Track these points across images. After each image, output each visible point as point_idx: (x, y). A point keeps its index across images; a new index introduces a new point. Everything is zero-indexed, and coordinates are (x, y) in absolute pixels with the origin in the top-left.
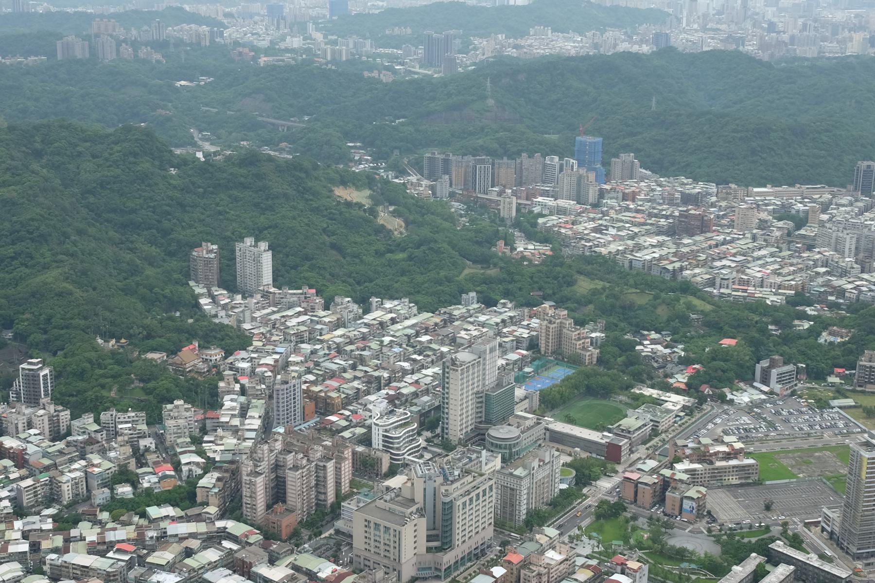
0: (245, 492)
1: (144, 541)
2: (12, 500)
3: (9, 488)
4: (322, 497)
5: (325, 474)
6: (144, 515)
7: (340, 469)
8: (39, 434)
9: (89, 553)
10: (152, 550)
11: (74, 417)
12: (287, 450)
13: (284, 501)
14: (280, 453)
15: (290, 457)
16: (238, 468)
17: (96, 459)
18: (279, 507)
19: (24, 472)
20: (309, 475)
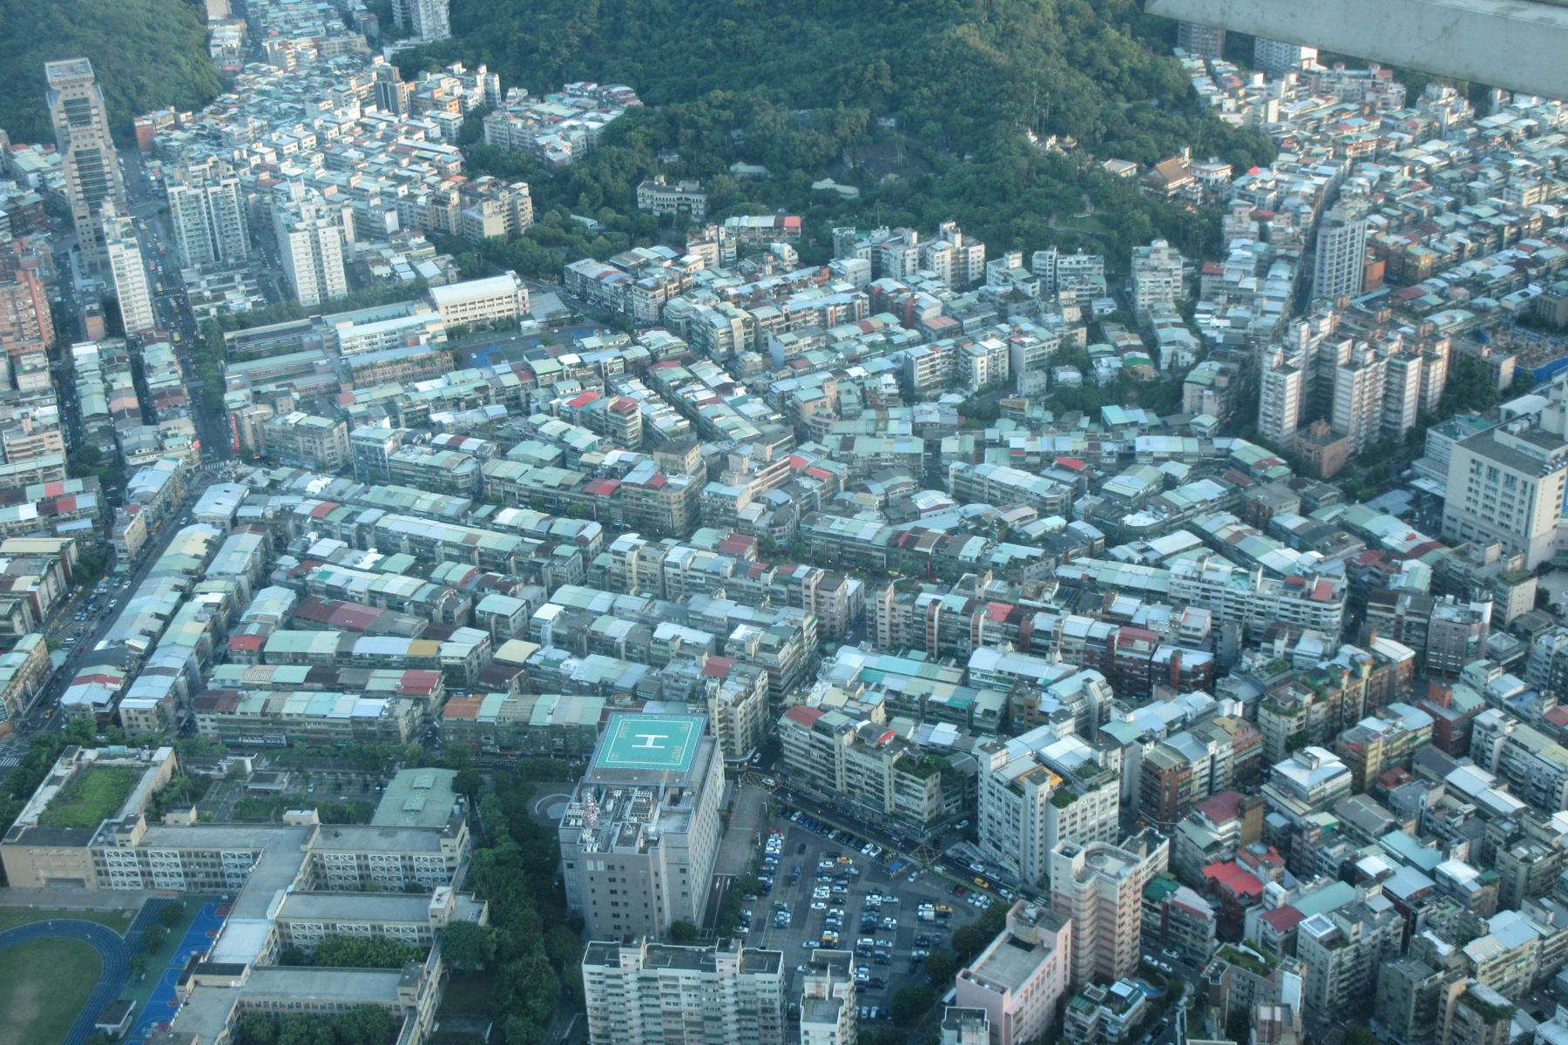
0: (1266, 398)
1: (1098, 457)
2: (898, 374)
3: (893, 356)
4: (1392, 417)
5: (1403, 378)
6: (1096, 416)
7: (1427, 374)
8: (937, 278)
9: (1013, 466)
10: (1112, 472)
11: (991, 255)
12: (1340, 334)
13: (1329, 420)
14: (1327, 339)
15: (1344, 348)
16: (1252, 357)
17: (1026, 325)
18: (1320, 428)
19: (913, 334)
20: (1375, 379)
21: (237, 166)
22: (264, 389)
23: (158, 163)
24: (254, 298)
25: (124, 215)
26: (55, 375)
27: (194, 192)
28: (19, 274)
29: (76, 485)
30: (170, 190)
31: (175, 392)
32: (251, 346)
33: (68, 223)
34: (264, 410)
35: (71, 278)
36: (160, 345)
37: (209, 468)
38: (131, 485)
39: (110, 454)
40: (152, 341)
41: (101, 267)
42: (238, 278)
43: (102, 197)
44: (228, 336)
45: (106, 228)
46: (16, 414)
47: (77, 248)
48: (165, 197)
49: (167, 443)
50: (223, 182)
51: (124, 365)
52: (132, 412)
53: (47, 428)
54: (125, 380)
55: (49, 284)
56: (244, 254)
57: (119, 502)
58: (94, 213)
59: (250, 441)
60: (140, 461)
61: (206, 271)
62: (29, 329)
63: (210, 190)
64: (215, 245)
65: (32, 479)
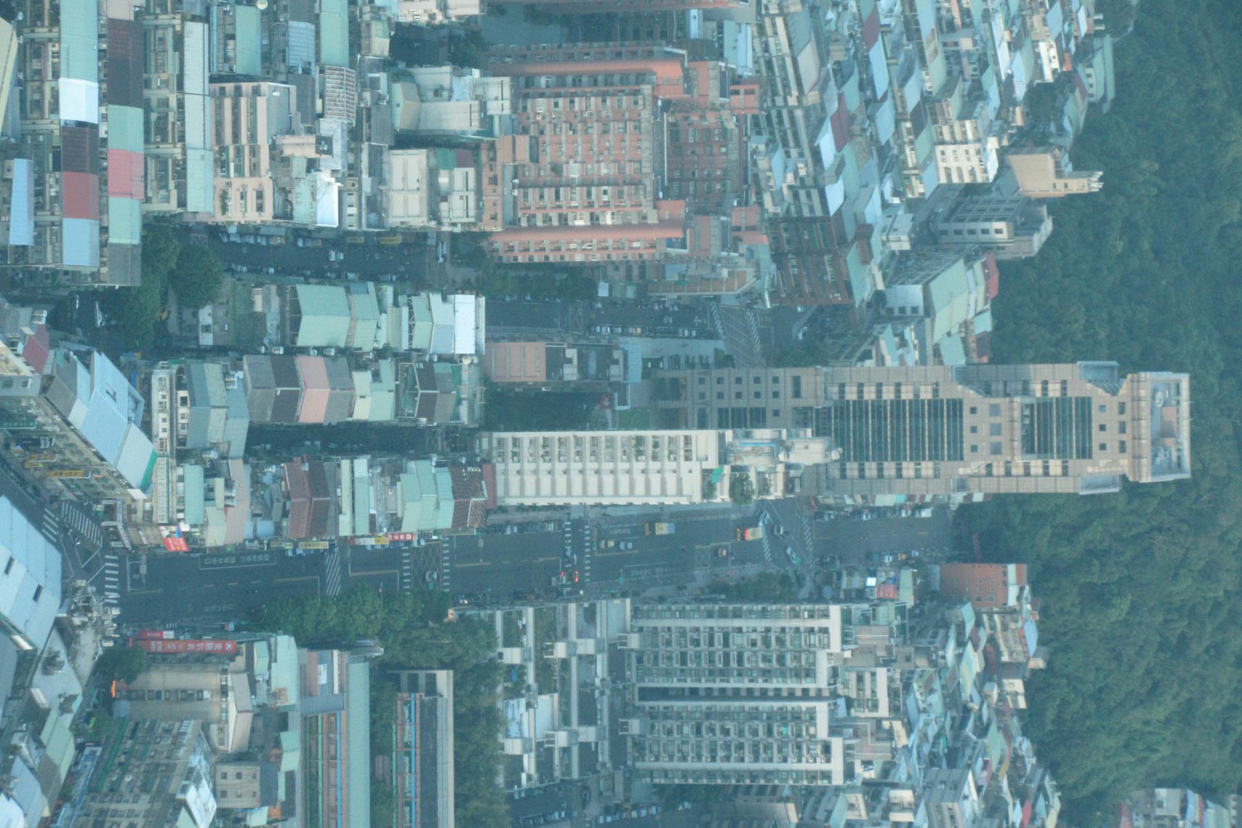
21: (873, 790)
22: (291, 740)
23: (908, 598)
24: (529, 763)
25: (789, 484)
26: (416, 240)
27: (823, 667)
28: (678, 209)
29: (125, 227)
30: (835, 610)
31: (322, 518)
32: (409, 732)
33: (784, 354)
34: (236, 727)
35: (652, 331)
36: (448, 508)
37: (110, 565)
38: (101, 361)
39: (193, 329)
40: (462, 490)
41: (667, 404)
42: (588, 734)
43: (841, 440)
44: (444, 680)
45: (763, 434)
46: (333, 126)
47: (725, 361)
48: (818, 597)
49: (193, 473)
50: (837, 744)
51: (411, 410)
52: (290, 402)
53: (284, 192)
54: (373, 403)
55: (645, 275)
56: (649, 763)
57: (61, 323)
58: (803, 417)
59: (159, 679)
60: (158, 396)
61: (617, 657)
62: (539, 203)
63: (822, 709)
64: (680, 694)
65: (162, 127)
